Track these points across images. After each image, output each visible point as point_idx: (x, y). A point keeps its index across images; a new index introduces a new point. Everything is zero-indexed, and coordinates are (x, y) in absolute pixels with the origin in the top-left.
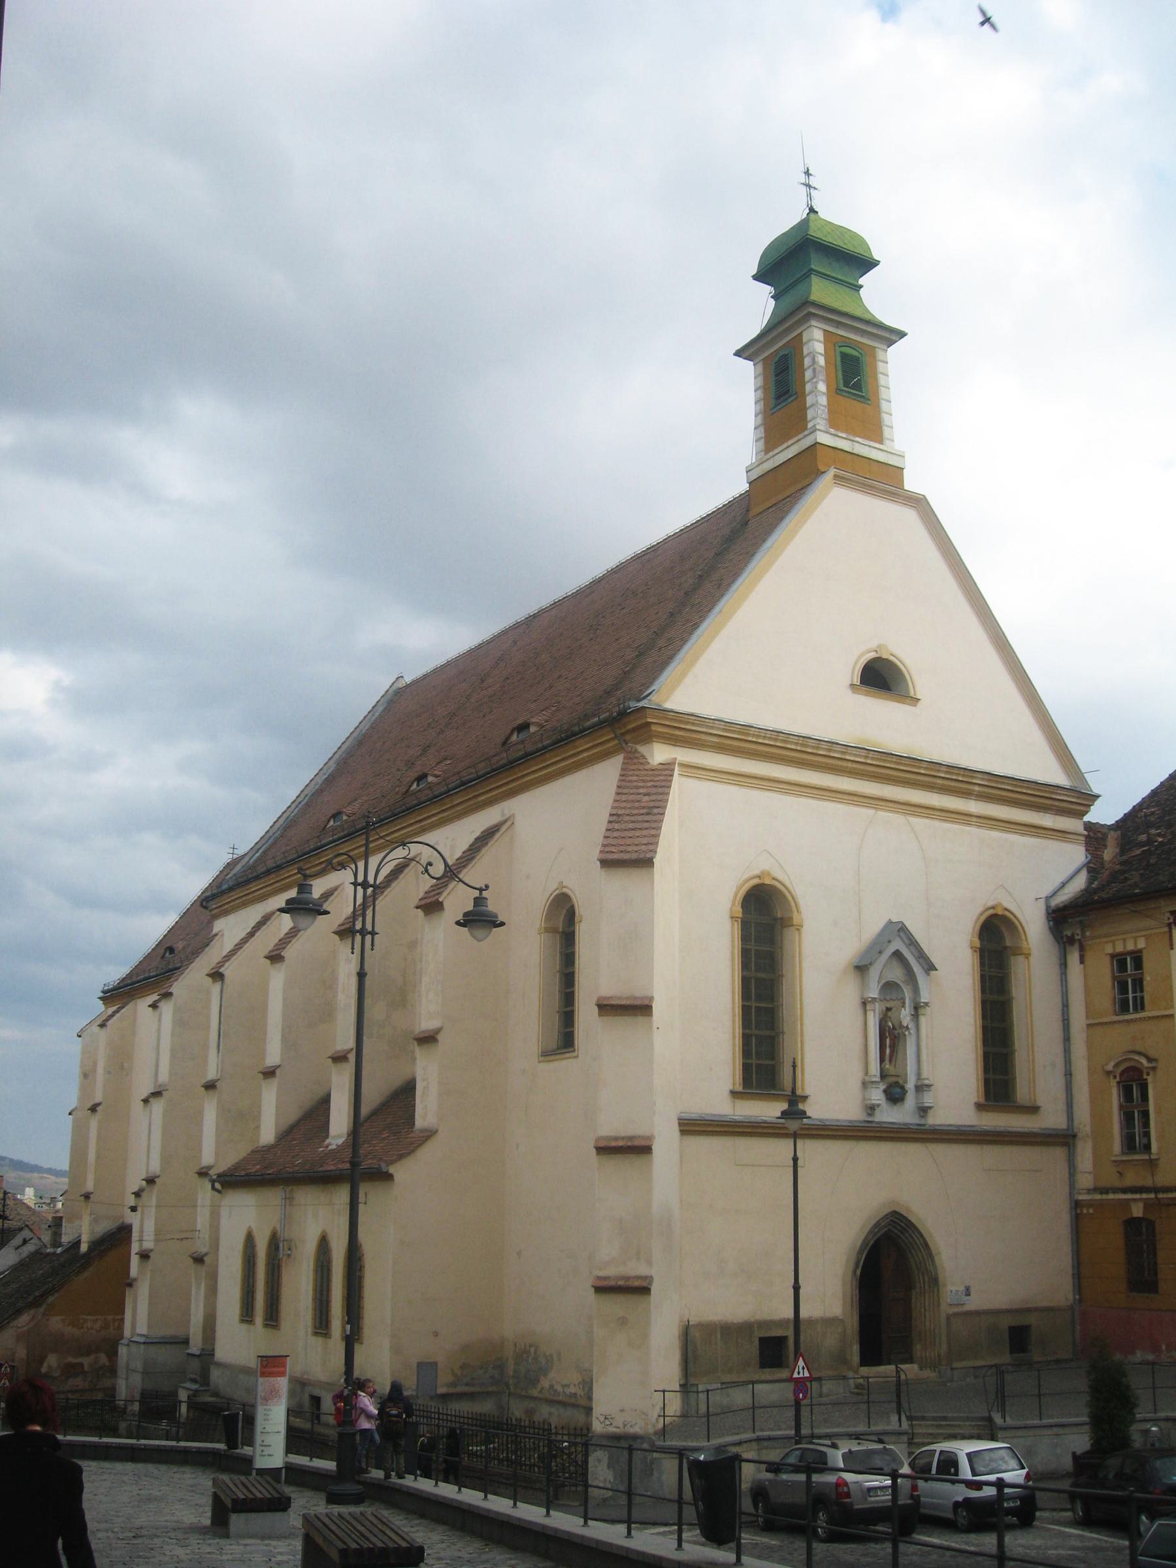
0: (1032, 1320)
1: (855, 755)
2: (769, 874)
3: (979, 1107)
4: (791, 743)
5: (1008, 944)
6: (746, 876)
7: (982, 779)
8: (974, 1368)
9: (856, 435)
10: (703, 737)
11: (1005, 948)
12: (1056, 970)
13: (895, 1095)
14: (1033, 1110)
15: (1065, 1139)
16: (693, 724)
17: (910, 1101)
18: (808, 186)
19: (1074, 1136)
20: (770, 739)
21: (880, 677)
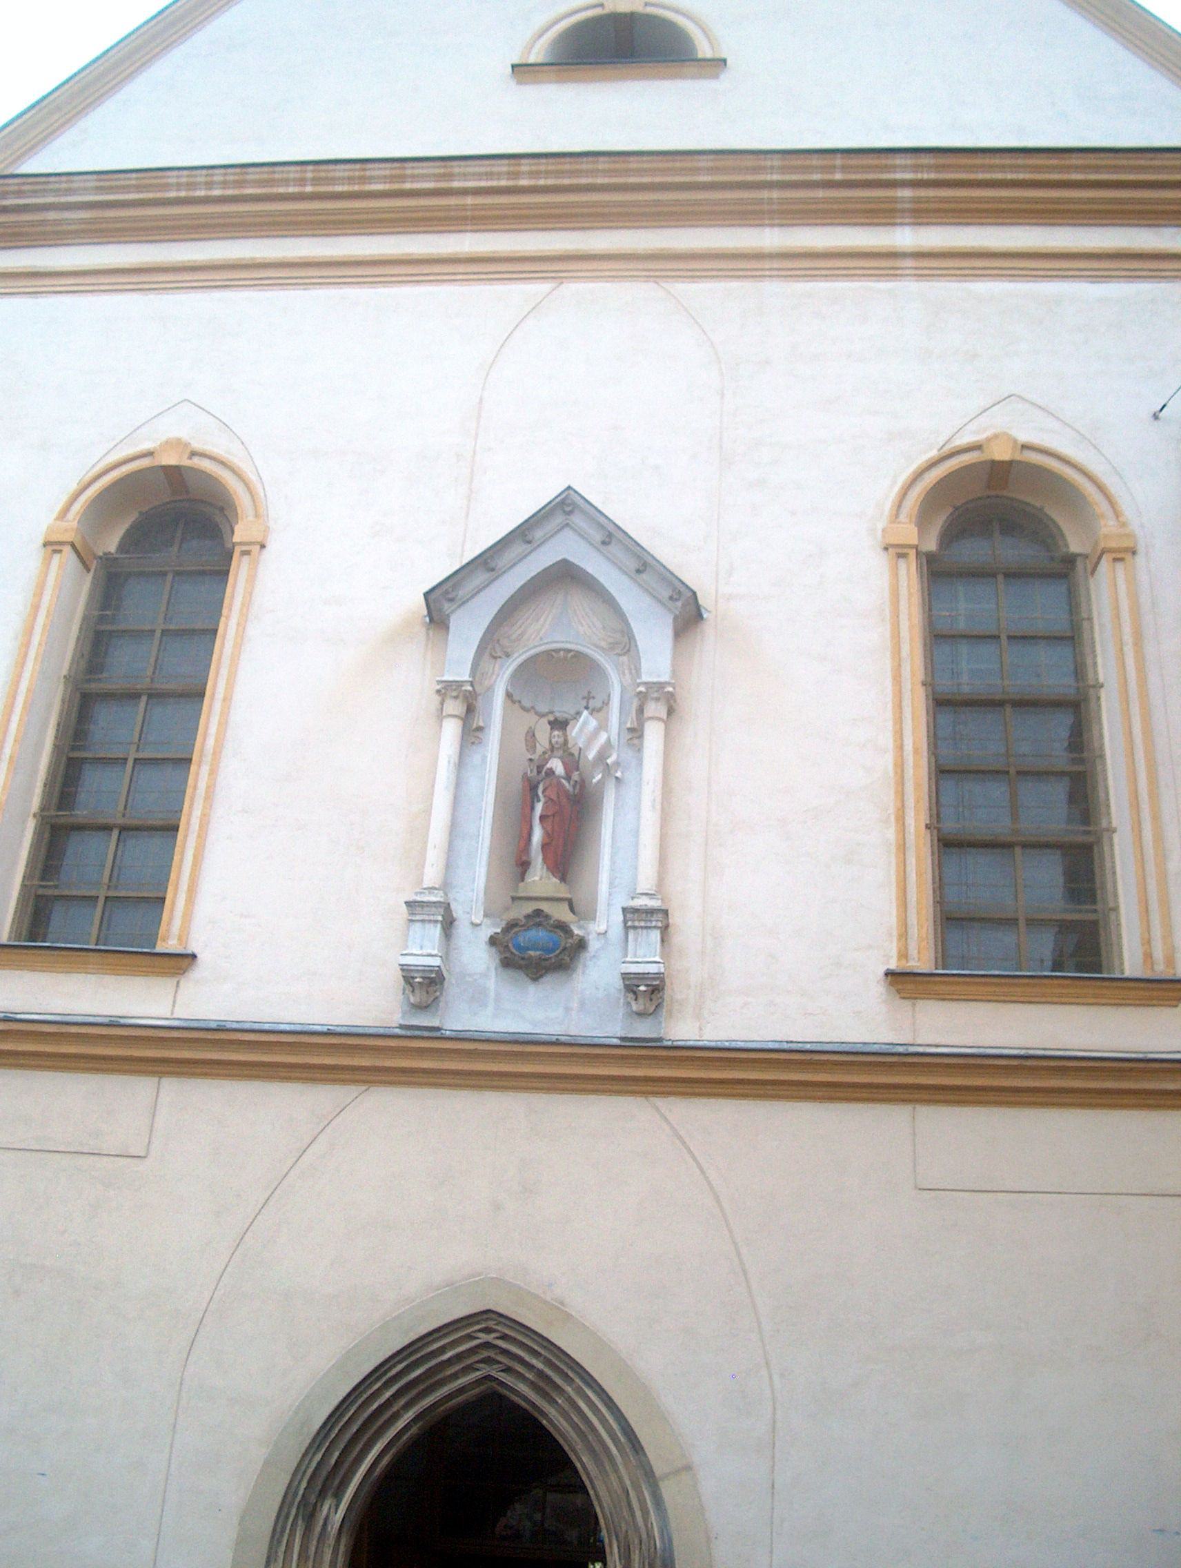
1: (479, 176)
2: (178, 444)
4: (286, 182)
5: (1075, 547)
7: (916, 168)
10: (52, 215)
11: (1070, 561)
13: (539, 948)
16: (19, 194)
17: (600, 973)
20: (225, 184)
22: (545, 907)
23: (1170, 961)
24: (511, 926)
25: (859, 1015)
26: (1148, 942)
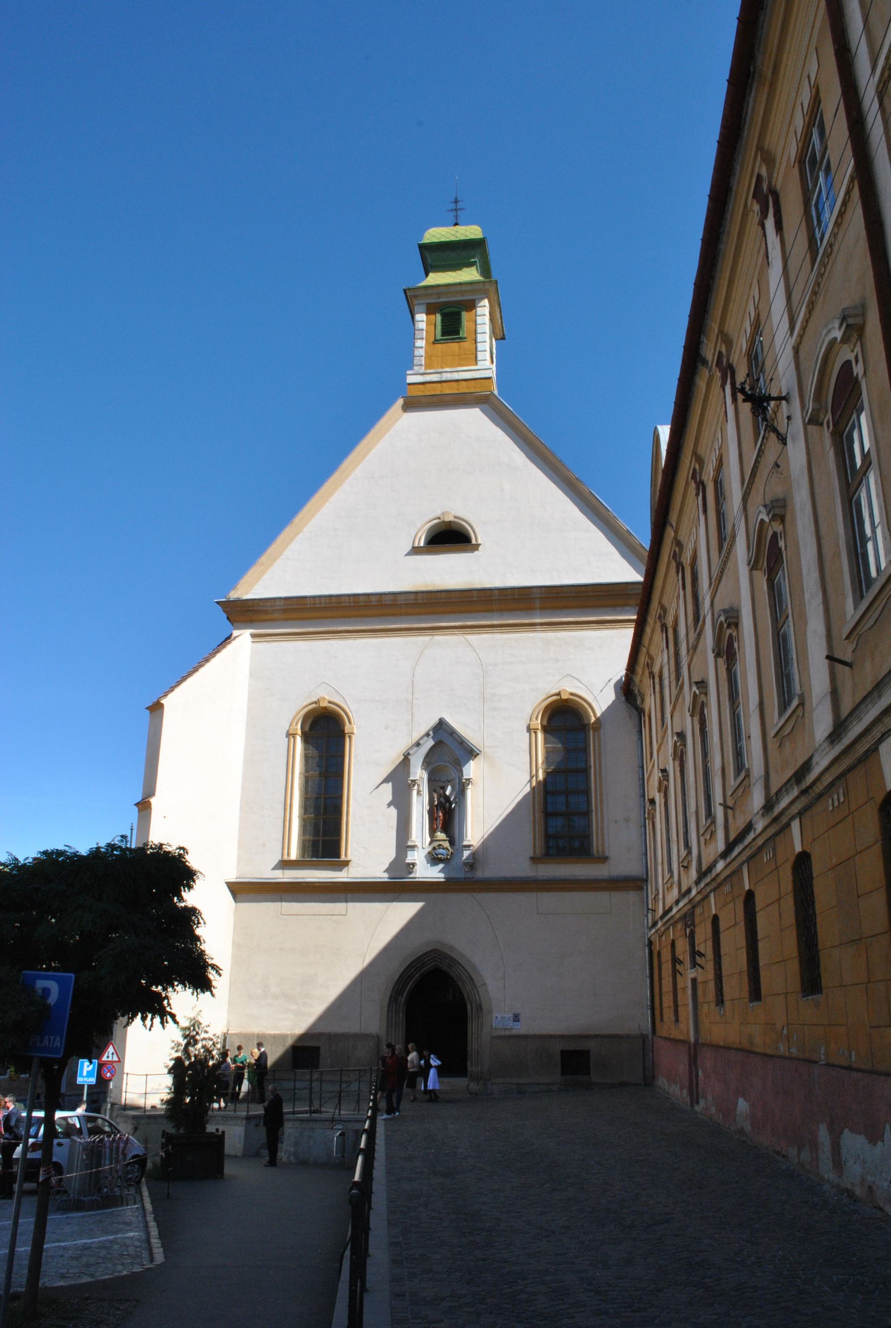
0: (591, 1045)
2: (324, 699)
3: (534, 860)
6: (305, 704)
8: (518, 1084)
9: (442, 368)
12: (635, 737)
14: (604, 859)
15: (637, 883)
18: (456, 210)
19: (647, 880)
21: (449, 537)
22: (441, 843)
23: (603, 852)
24: (434, 848)
25: (522, 868)
26: (597, 847)
